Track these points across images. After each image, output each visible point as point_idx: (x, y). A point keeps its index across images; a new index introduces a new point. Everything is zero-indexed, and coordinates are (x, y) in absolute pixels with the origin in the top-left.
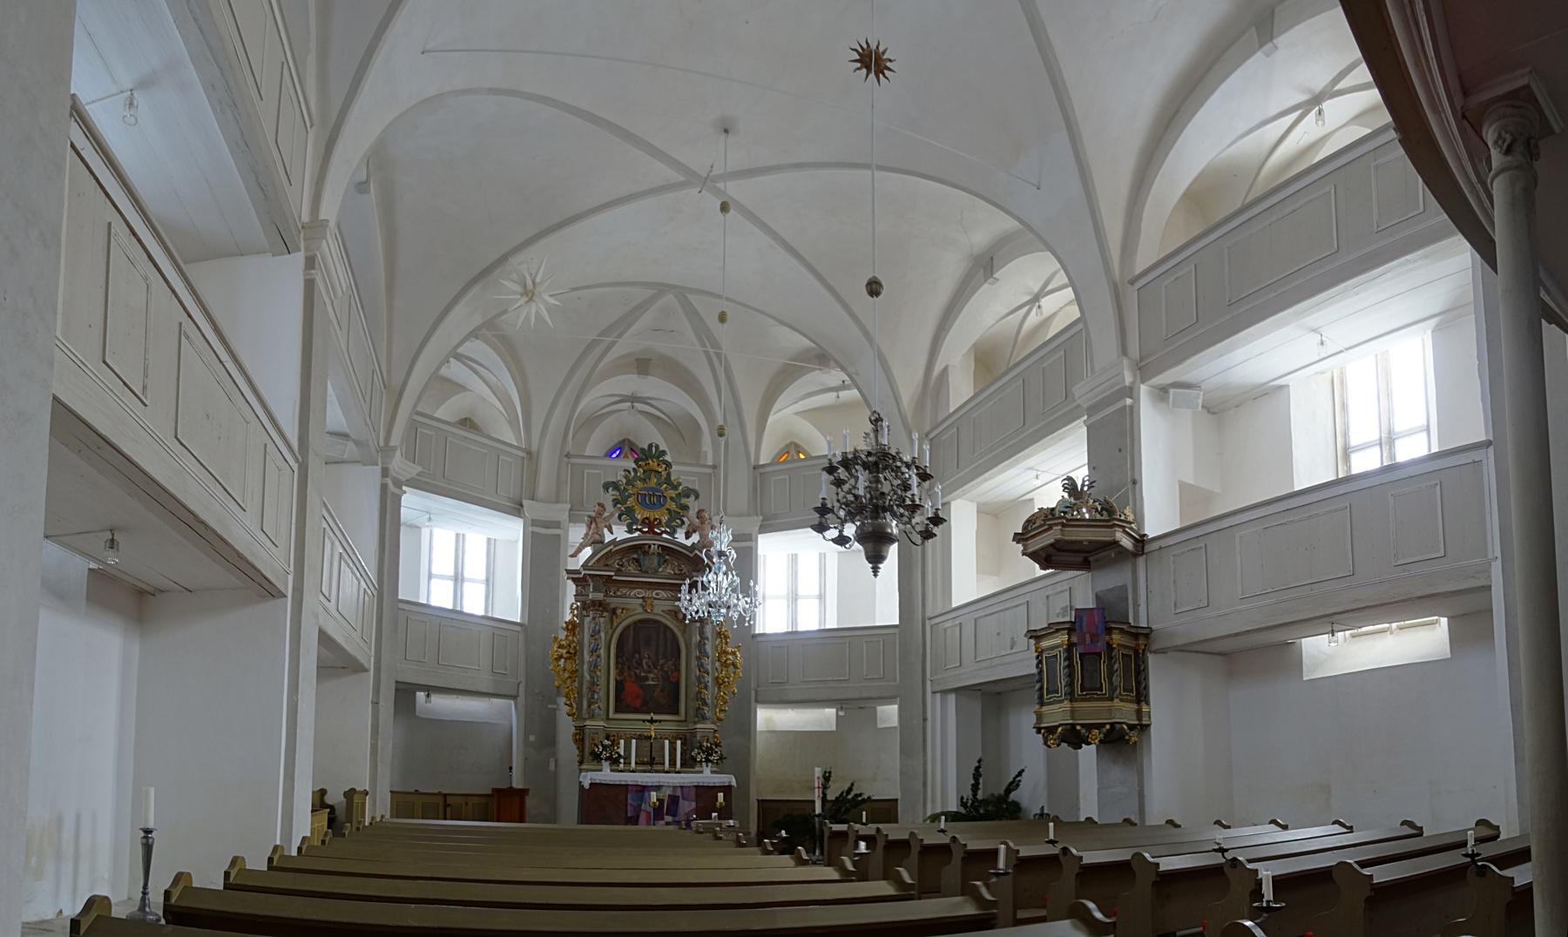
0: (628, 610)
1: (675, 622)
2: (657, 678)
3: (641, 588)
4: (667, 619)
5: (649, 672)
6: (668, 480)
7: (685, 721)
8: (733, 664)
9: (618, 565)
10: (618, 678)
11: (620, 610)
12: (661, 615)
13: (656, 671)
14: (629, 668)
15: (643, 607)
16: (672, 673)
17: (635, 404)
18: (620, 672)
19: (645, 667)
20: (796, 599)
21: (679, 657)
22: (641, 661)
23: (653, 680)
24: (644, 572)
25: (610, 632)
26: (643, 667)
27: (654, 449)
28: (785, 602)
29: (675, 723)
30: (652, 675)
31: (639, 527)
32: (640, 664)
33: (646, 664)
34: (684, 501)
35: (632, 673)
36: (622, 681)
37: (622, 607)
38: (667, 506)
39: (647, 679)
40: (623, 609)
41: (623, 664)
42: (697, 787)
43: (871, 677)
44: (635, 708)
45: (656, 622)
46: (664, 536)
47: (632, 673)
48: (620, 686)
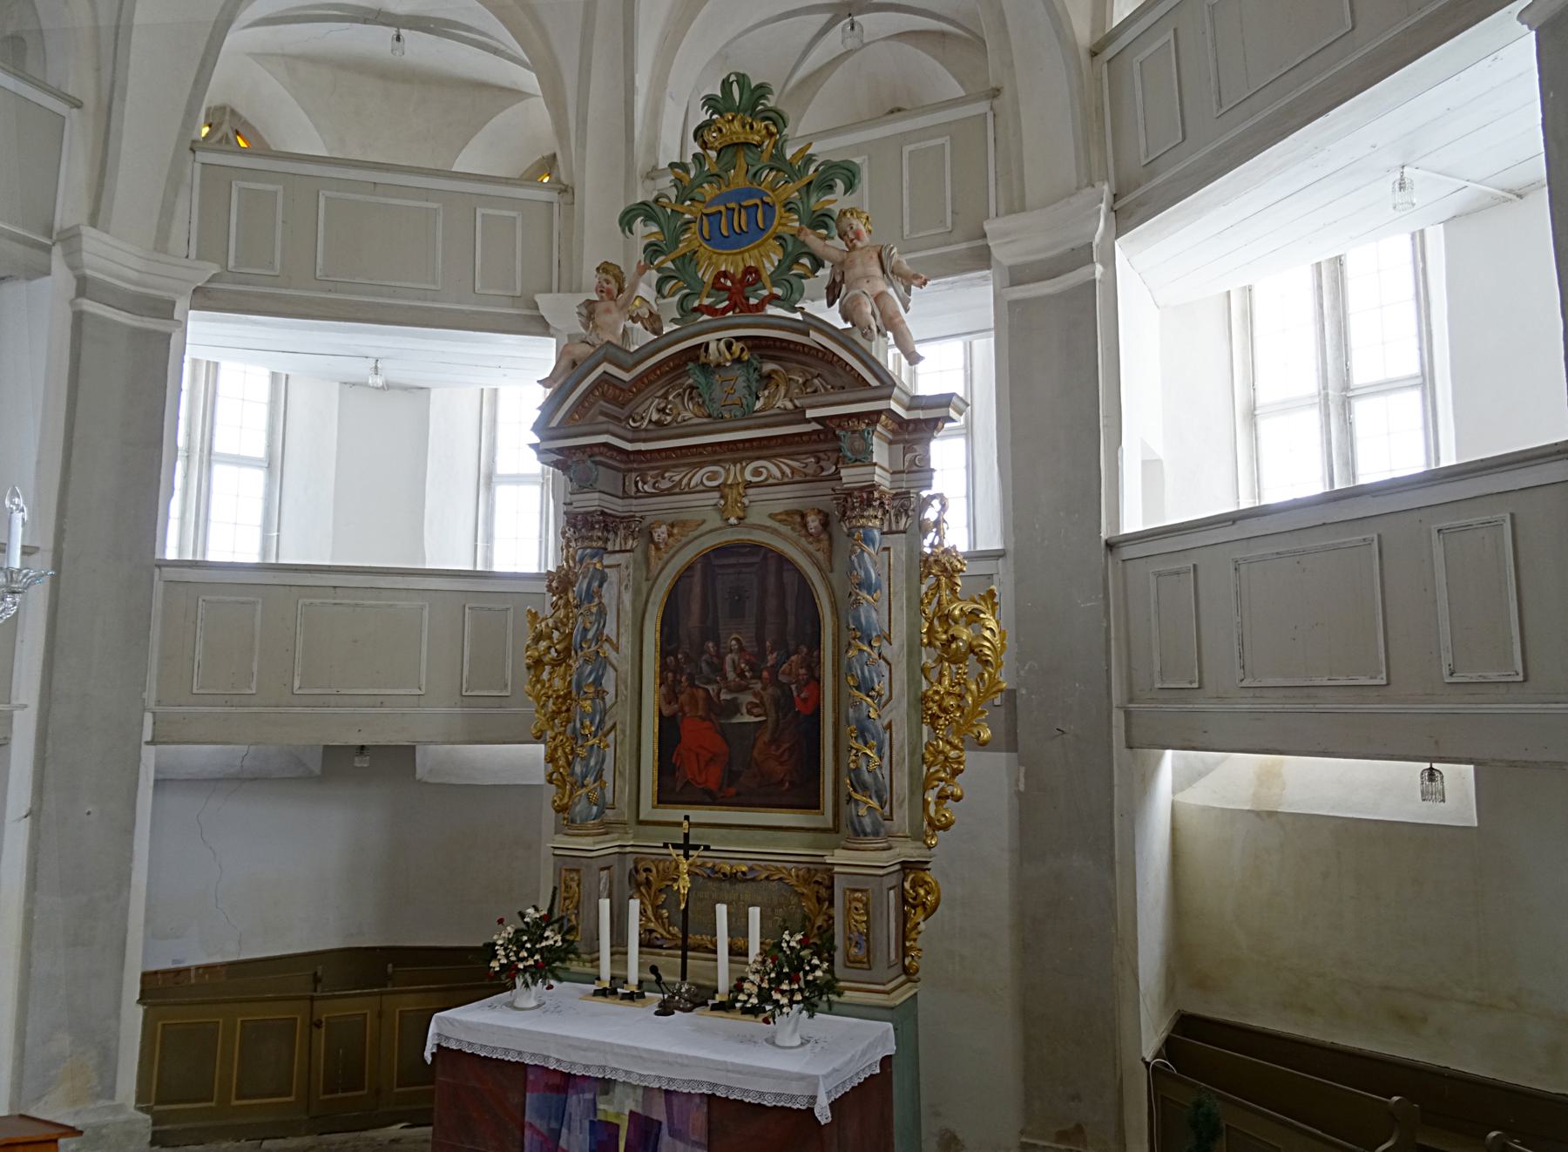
0: (683, 524)
1: (803, 541)
2: (762, 704)
3: (758, 458)
4: (785, 538)
5: (743, 689)
6: (778, 163)
7: (835, 829)
8: (971, 649)
9: (659, 411)
10: (666, 712)
11: (664, 528)
12: (764, 528)
13: (758, 686)
14: (691, 678)
15: (722, 511)
16: (800, 690)
17: (856, 18)
18: (670, 692)
19: (731, 675)
20: (1346, 405)
21: (816, 643)
22: (722, 658)
23: (749, 712)
24: (716, 420)
25: (645, 587)
26: (725, 677)
27: (735, 88)
28: (1313, 417)
29: (809, 836)
30: (747, 698)
31: (707, 301)
32: (719, 669)
33: (735, 666)
34: (816, 202)
35: (701, 693)
36: (674, 716)
37: (671, 518)
38: (776, 227)
39: (734, 708)
40: (672, 525)
41: (677, 670)
42: (711, 1098)
43: (1473, 676)
44: (709, 793)
45: (756, 548)
46: (771, 310)
47: (701, 693)
48: (669, 730)
